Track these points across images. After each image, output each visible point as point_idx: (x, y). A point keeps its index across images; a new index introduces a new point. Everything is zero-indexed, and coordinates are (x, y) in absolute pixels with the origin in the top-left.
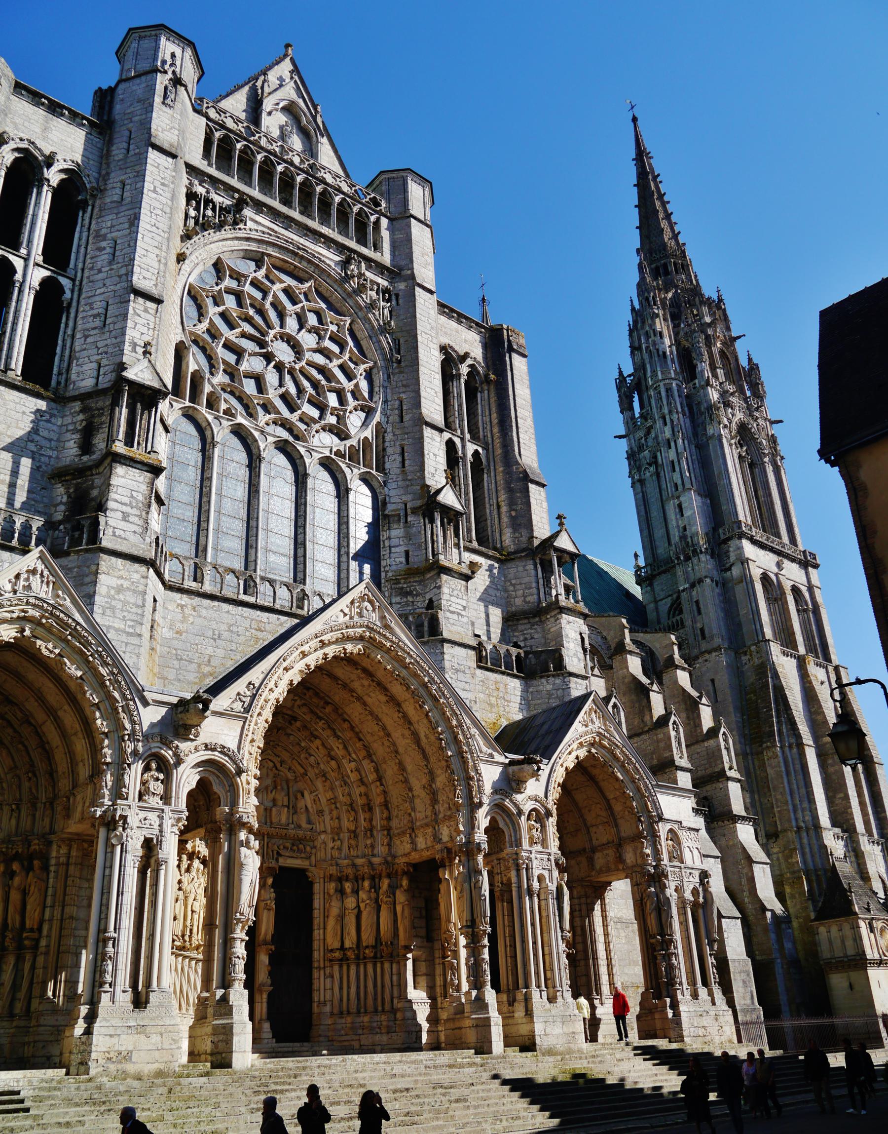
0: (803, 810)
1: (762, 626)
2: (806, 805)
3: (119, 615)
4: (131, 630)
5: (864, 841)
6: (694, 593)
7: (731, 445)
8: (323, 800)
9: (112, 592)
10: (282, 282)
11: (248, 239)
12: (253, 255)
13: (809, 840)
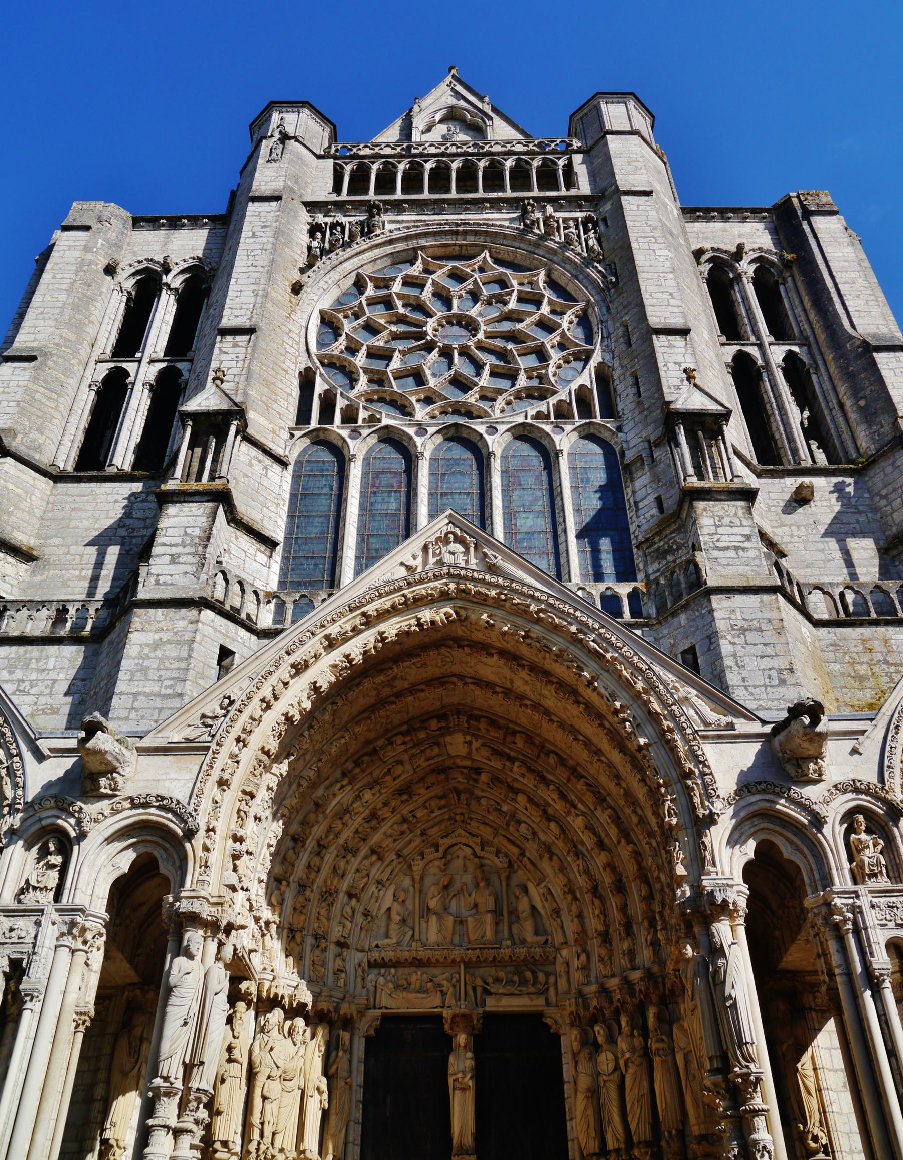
3: (153, 675)
4: (169, 691)
8: (557, 891)
9: (147, 650)
10: (441, 267)
11: (391, 242)
12: (403, 256)
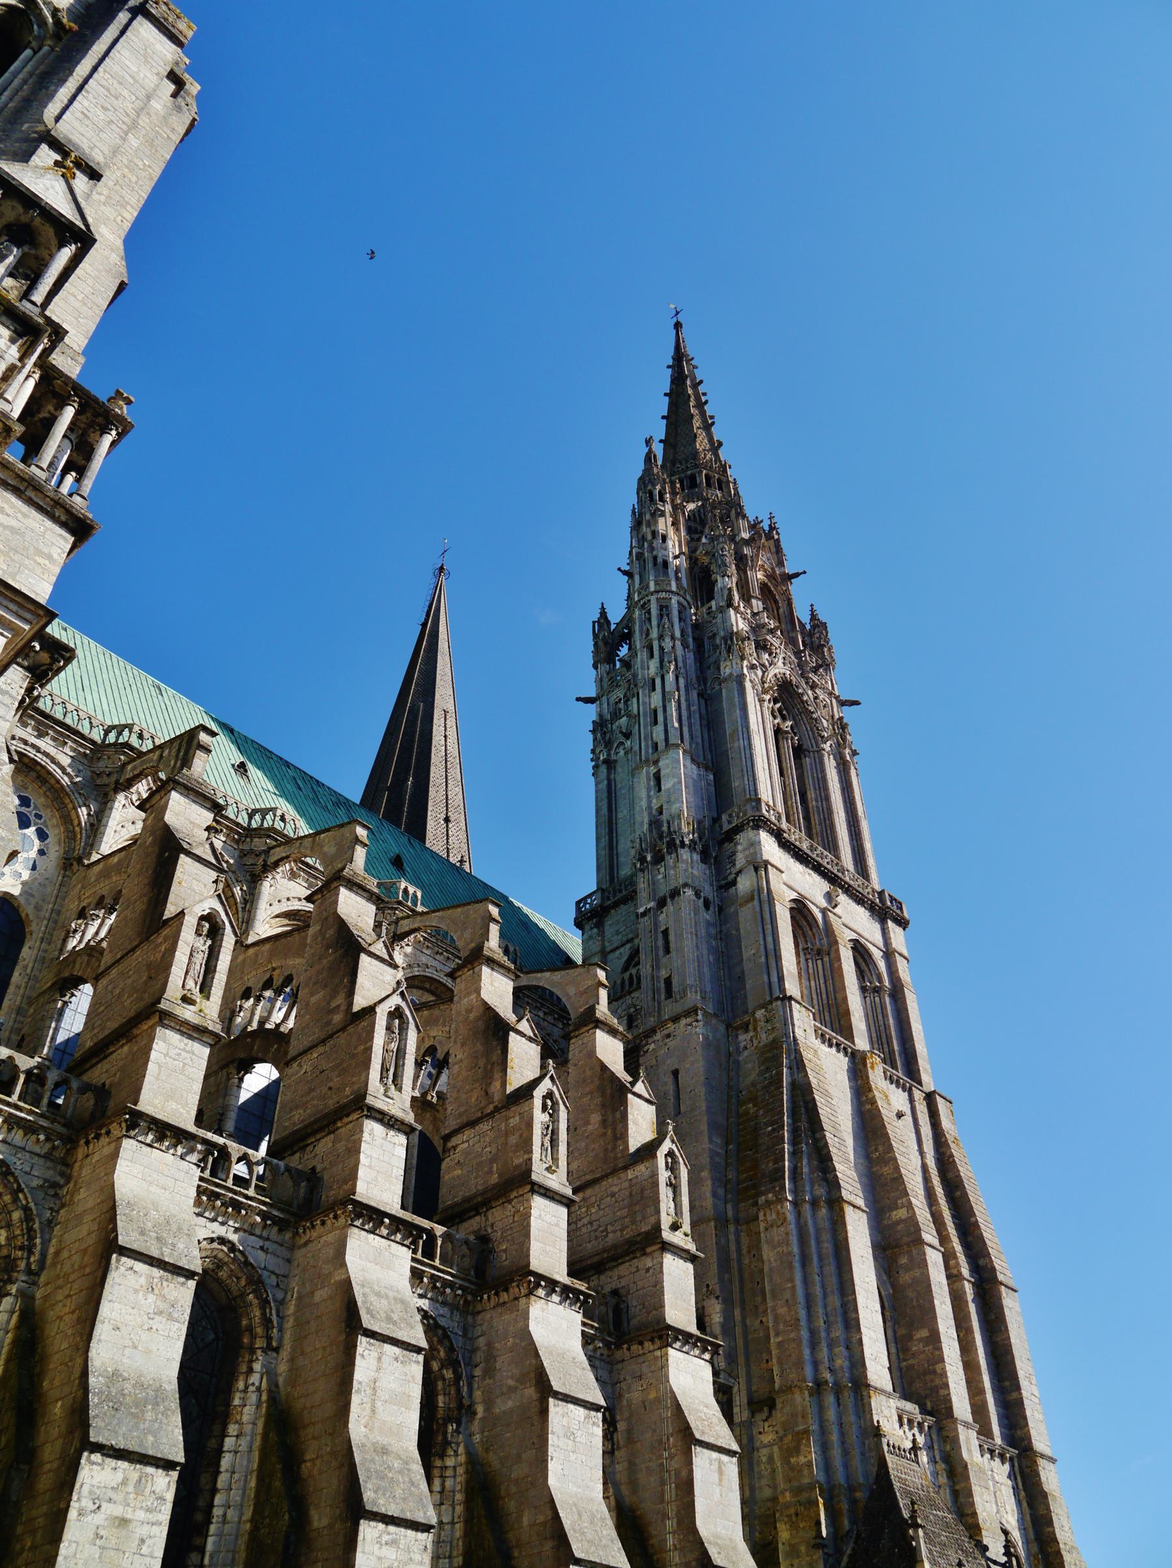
0: (831, 1346)
1: (781, 979)
2: (838, 1332)
5: (969, 1442)
6: (662, 917)
7: (761, 701)
13: (840, 1416)
